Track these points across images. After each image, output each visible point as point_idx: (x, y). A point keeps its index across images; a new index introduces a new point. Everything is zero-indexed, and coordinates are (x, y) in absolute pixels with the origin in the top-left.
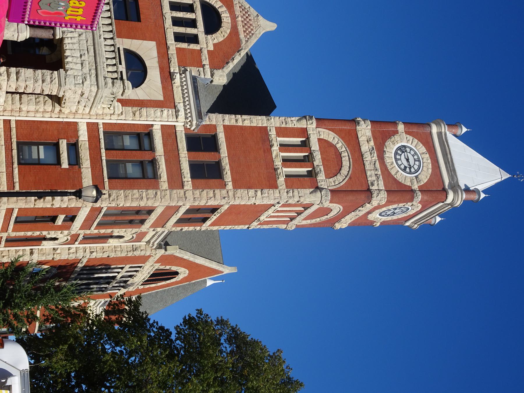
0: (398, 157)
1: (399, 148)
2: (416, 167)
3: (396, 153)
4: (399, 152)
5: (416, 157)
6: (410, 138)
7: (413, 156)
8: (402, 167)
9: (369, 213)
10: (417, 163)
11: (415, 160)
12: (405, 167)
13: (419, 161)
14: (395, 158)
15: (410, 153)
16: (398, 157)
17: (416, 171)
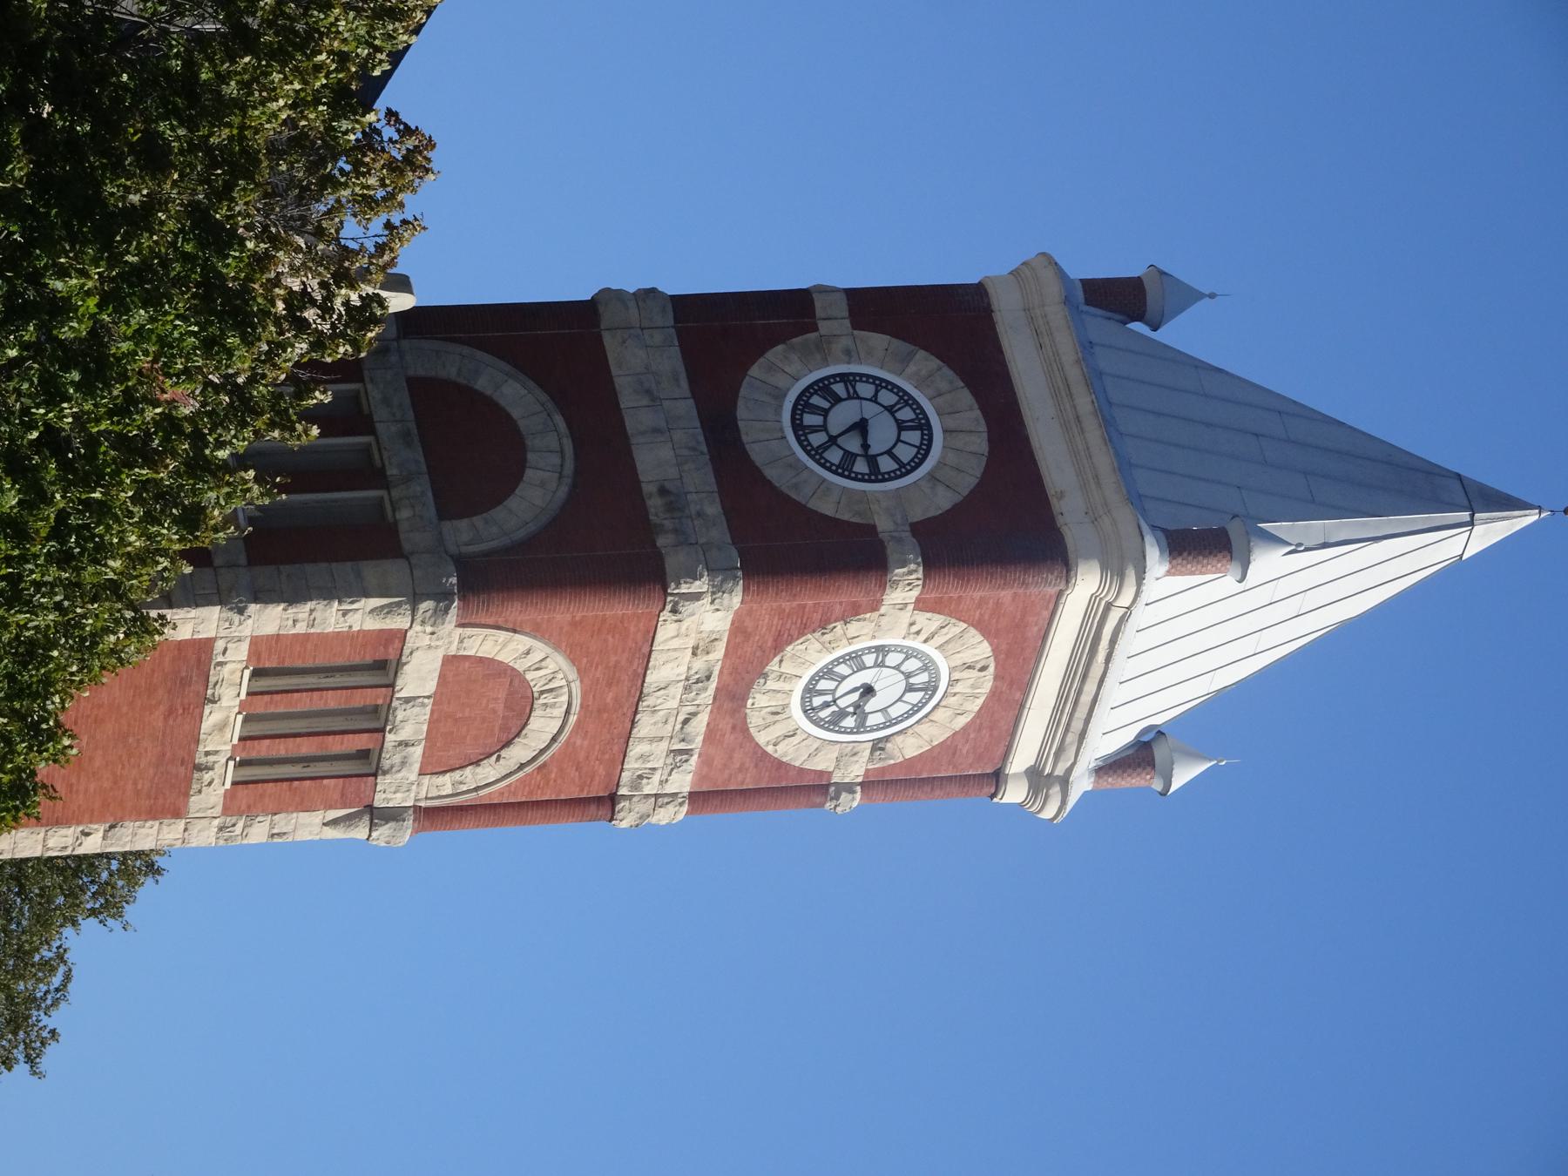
0: (810, 419)
1: (822, 387)
2: (906, 453)
3: (802, 405)
4: (816, 400)
5: (906, 414)
6: (879, 340)
7: (891, 410)
8: (834, 456)
9: (733, 695)
10: (914, 437)
11: (901, 426)
12: (849, 457)
13: (923, 425)
14: (797, 426)
15: (874, 399)
16: (810, 419)
17: (905, 469)
